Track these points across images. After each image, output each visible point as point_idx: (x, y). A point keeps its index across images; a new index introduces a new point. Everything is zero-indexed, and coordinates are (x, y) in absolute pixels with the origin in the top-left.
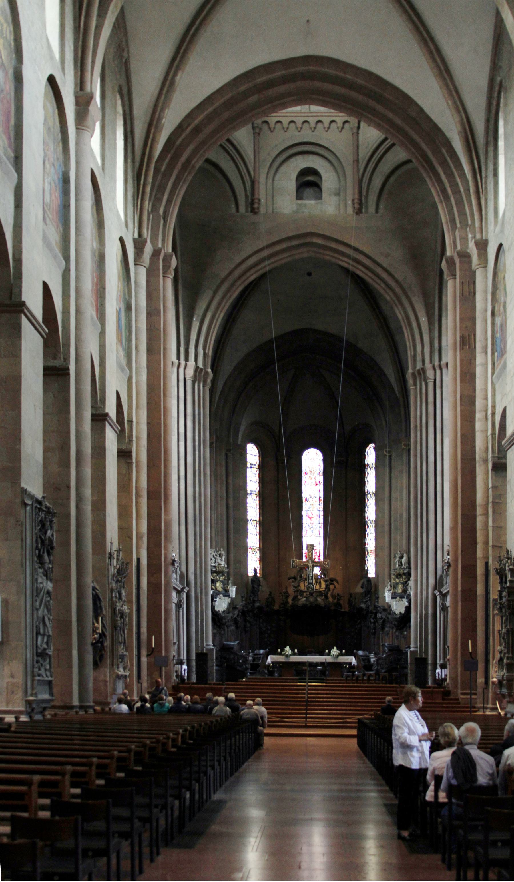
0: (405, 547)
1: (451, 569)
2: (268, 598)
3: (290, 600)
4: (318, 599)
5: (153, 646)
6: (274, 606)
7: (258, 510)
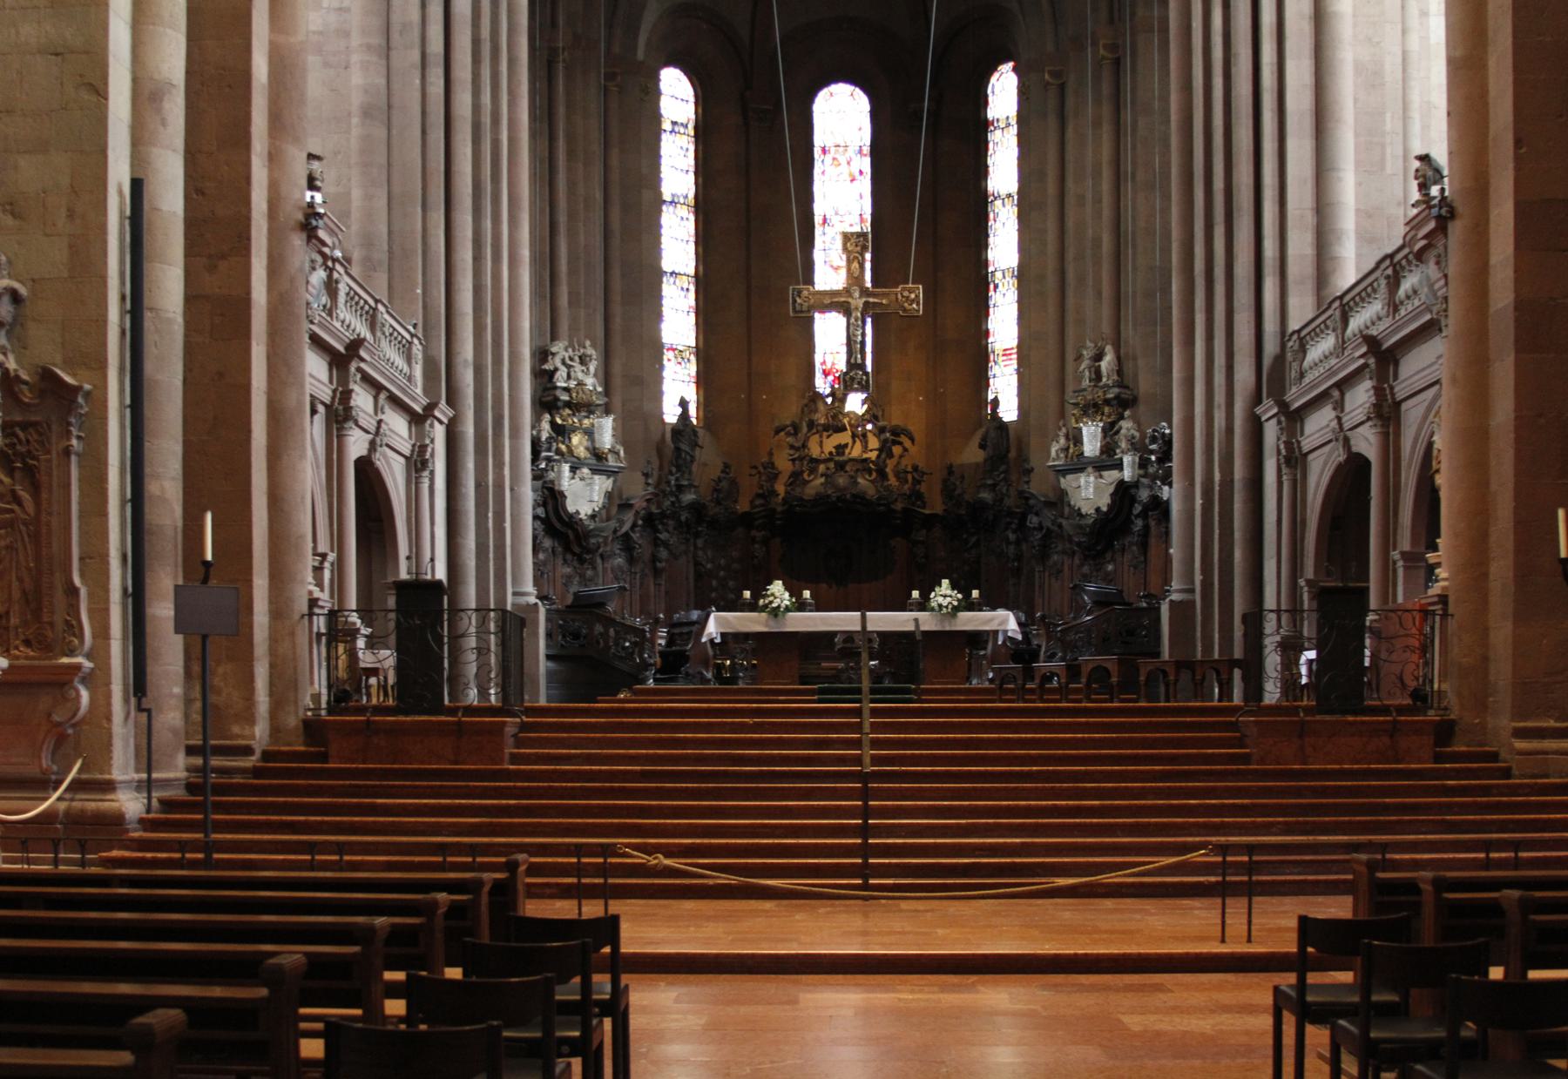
0: (1106, 328)
1: (1456, 229)
2: (720, 480)
3: (780, 488)
4: (860, 480)
5: (209, 557)
6: (736, 502)
7: (692, 247)
